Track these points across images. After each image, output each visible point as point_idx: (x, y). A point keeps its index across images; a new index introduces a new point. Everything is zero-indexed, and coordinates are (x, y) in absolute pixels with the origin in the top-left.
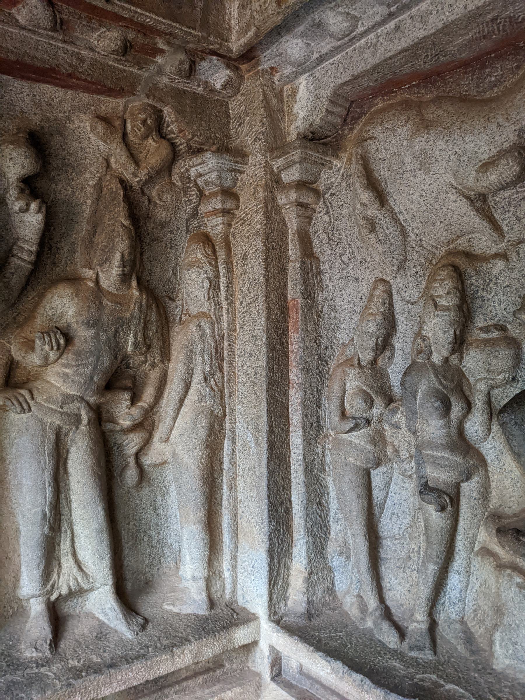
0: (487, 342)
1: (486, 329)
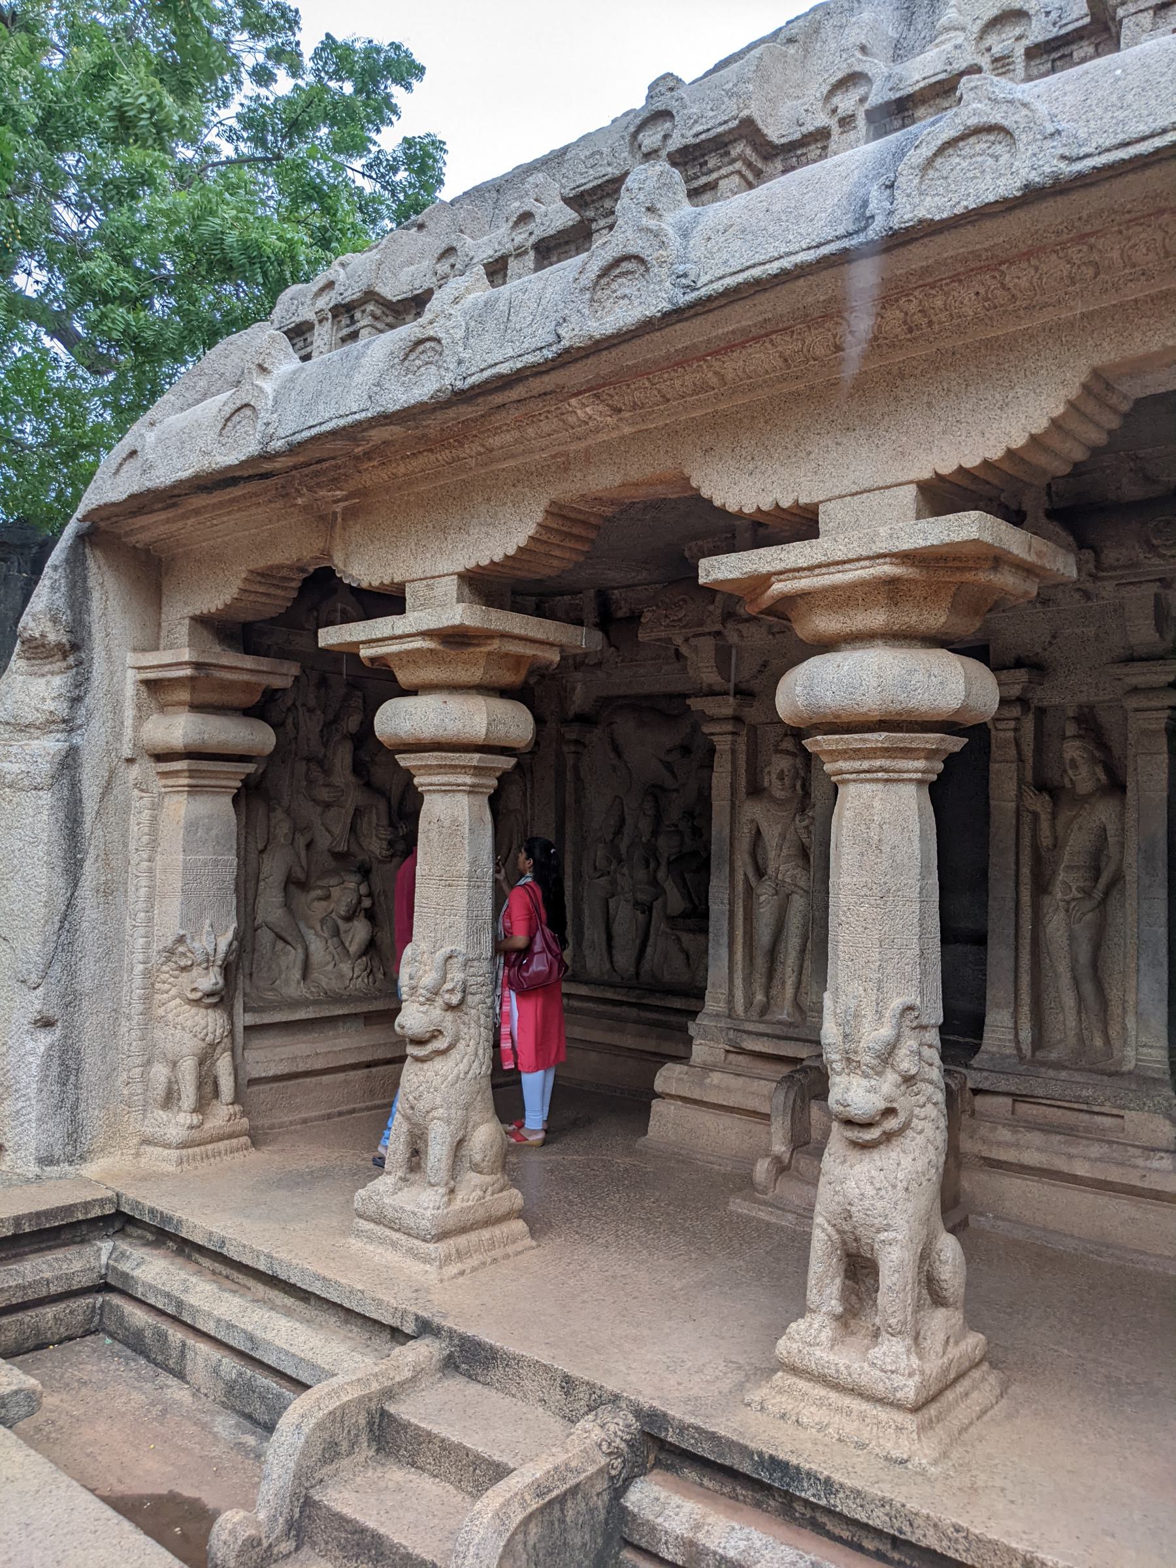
0: (670, 832)
1: (668, 826)
